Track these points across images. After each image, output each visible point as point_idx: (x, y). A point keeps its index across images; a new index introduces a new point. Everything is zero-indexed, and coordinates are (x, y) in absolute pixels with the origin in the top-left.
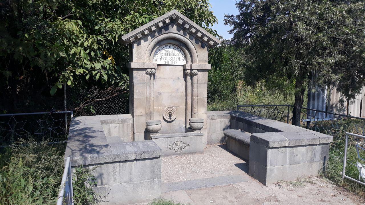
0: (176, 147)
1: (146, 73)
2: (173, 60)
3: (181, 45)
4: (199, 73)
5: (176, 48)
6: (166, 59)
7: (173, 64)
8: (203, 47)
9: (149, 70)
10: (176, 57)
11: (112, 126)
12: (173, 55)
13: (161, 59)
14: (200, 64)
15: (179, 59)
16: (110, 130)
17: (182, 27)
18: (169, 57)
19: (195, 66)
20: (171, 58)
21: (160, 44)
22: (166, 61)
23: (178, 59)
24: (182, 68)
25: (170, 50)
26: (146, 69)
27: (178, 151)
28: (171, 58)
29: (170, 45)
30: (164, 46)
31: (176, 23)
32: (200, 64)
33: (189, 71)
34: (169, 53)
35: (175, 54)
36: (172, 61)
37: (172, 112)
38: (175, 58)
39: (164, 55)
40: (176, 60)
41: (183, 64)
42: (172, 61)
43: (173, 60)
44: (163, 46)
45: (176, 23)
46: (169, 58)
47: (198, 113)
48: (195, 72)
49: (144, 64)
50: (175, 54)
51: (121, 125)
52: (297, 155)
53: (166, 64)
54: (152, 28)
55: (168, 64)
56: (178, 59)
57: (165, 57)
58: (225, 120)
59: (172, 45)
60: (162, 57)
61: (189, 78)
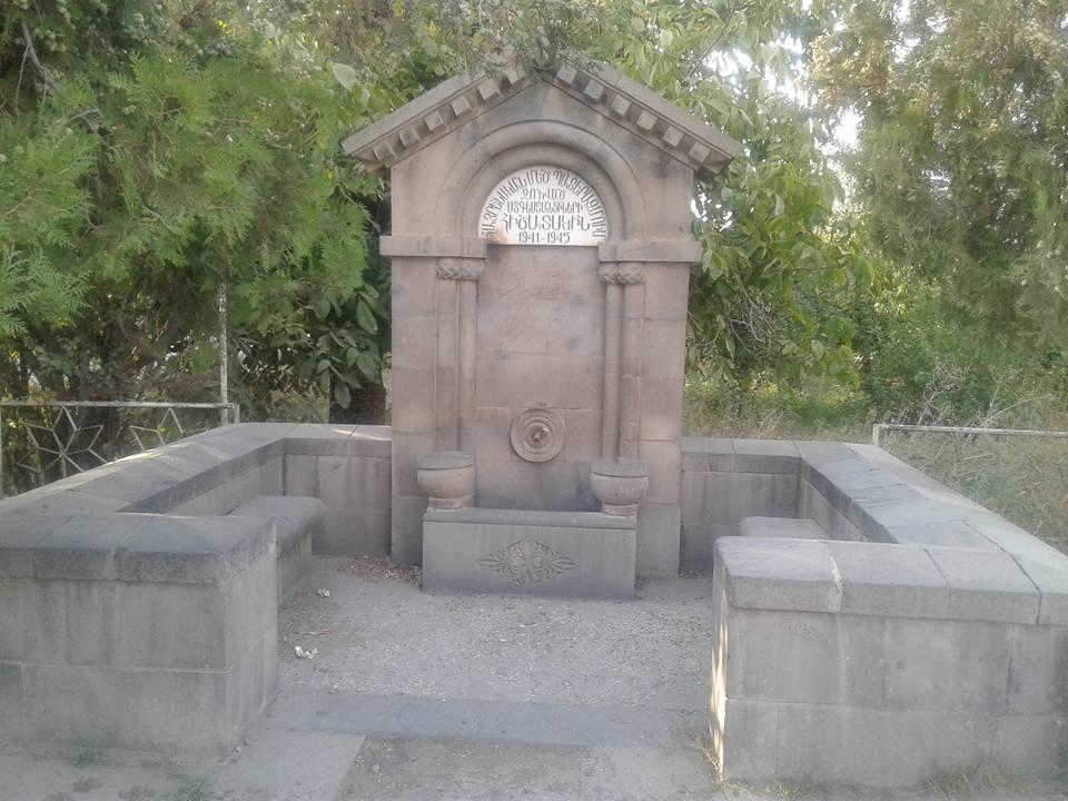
0: (516, 562)
1: (438, 273)
2: (556, 226)
3: (584, 165)
4: (653, 277)
5: (568, 182)
6: (528, 225)
7: (557, 243)
8: (662, 170)
9: (447, 265)
10: (568, 217)
11: (325, 460)
12: (558, 210)
13: (508, 225)
14: (655, 239)
15: (581, 223)
16: (316, 474)
17: (577, 95)
18: (540, 216)
19: (630, 248)
20: (547, 219)
21: (500, 163)
22: (530, 232)
23: (575, 222)
24: (585, 260)
25: (543, 188)
26: (438, 258)
27: (527, 578)
28: (547, 218)
29: (546, 169)
30: (522, 175)
31: (556, 82)
32: (655, 239)
33: (608, 270)
34: (541, 200)
35: (566, 205)
36: (551, 230)
37: (546, 429)
38: (566, 221)
39: (521, 210)
40: (566, 226)
41: (595, 244)
42: (551, 230)
43: (556, 226)
44: (516, 175)
45: (556, 82)
46: (540, 221)
47: (643, 436)
48: (629, 271)
49: (428, 240)
50: (566, 205)
51: (355, 460)
52: (900, 665)
53: (529, 242)
54: (454, 105)
55: (535, 243)
56: (575, 222)
57: (526, 215)
58: (773, 480)
59: (553, 170)
60: (514, 215)
61: (613, 291)
